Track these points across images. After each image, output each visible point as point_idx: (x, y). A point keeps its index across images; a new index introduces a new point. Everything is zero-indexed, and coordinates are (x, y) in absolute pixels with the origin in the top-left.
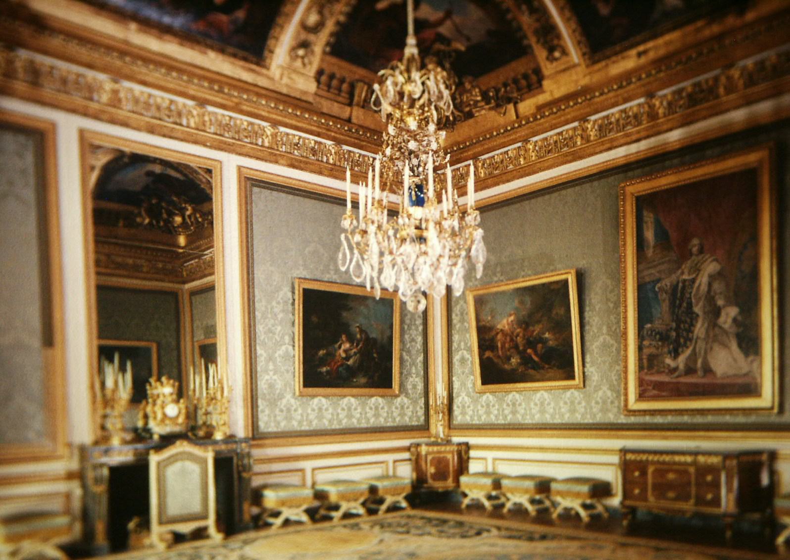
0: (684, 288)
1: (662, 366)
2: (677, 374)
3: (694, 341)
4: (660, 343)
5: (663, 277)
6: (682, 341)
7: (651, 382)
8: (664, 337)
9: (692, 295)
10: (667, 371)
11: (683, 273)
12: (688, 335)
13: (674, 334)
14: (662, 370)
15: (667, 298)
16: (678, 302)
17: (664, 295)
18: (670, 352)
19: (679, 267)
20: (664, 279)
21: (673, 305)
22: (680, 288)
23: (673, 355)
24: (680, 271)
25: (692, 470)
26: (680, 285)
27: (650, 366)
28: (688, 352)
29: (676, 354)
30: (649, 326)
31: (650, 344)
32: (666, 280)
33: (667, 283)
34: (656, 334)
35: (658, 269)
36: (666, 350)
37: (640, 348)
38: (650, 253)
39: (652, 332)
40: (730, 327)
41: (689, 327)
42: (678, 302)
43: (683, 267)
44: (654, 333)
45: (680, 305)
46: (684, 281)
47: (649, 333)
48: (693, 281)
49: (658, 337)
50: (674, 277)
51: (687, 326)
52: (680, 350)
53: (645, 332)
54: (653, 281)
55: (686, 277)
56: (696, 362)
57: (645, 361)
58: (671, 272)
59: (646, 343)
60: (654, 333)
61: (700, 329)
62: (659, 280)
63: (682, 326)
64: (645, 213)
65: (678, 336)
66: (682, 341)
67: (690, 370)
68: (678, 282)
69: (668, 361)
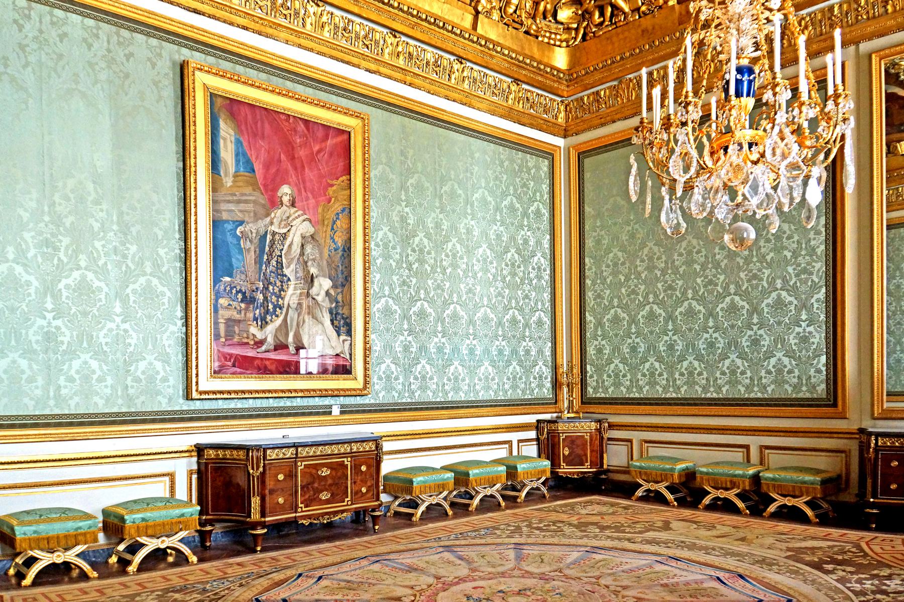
0: (273, 242)
1: (245, 335)
2: (264, 348)
3: (285, 310)
4: (243, 305)
5: (246, 219)
6: (271, 306)
7: (231, 355)
8: (248, 299)
9: (283, 252)
10: (252, 343)
11: (272, 223)
12: (278, 301)
13: (260, 297)
14: (246, 341)
15: (253, 248)
16: (265, 257)
17: (248, 243)
18: (256, 319)
19: (268, 215)
20: (248, 223)
21: (259, 261)
22: (268, 241)
23: (259, 323)
24: (268, 219)
25: (347, 462)
26: (269, 237)
27: (229, 335)
28: (279, 322)
29: (263, 323)
30: (228, 279)
31: (229, 305)
32: (250, 225)
33: (252, 228)
34: (237, 292)
35: (242, 206)
36: (250, 315)
37: (216, 309)
38: (228, 182)
39: (232, 288)
40: (323, 301)
41: (280, 291)
42: (265, 257)
43: (273, 215)
44: (234, 291)
45: (269, 261)
46: (274, 234)
47: (228, 288)
48: (284, 236)
49: (240, 296)
50: (261, 224)
51: (276, 290)
52: (269, 318)
53: (222, 288)
54: (234, 222)
55: (274, 228)
56: (287, 335)
57: (222, 327)
58: (257, 218)
59: (223, 301)
60: (234, 291)
61: (291, 296)
62: (241, 223)
63: (271, 288)
64: (222, 124)
65: (266, 298)
66: (271, 306)
67: (281, 347)
68: (266, 232)
69: (253, 330)
